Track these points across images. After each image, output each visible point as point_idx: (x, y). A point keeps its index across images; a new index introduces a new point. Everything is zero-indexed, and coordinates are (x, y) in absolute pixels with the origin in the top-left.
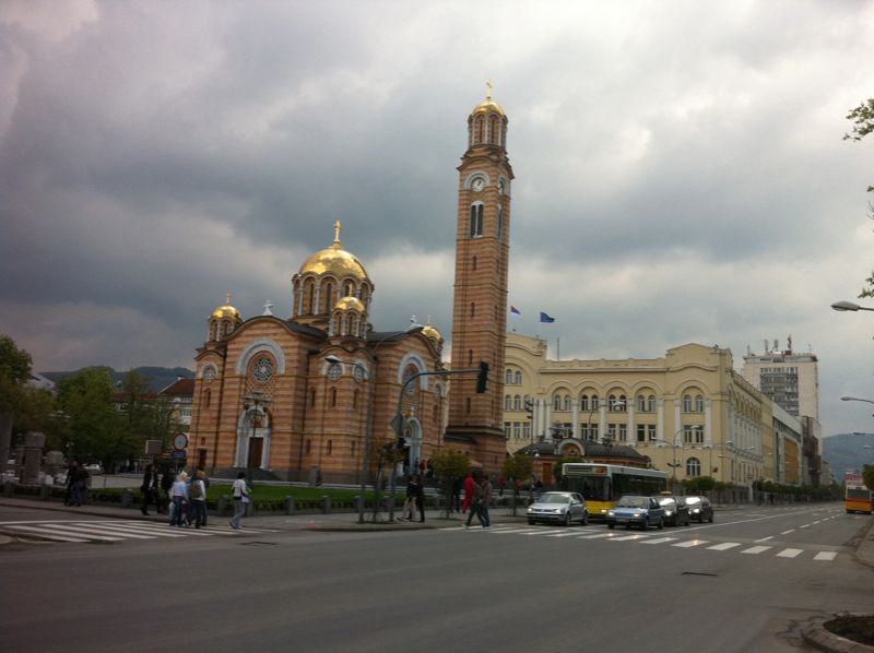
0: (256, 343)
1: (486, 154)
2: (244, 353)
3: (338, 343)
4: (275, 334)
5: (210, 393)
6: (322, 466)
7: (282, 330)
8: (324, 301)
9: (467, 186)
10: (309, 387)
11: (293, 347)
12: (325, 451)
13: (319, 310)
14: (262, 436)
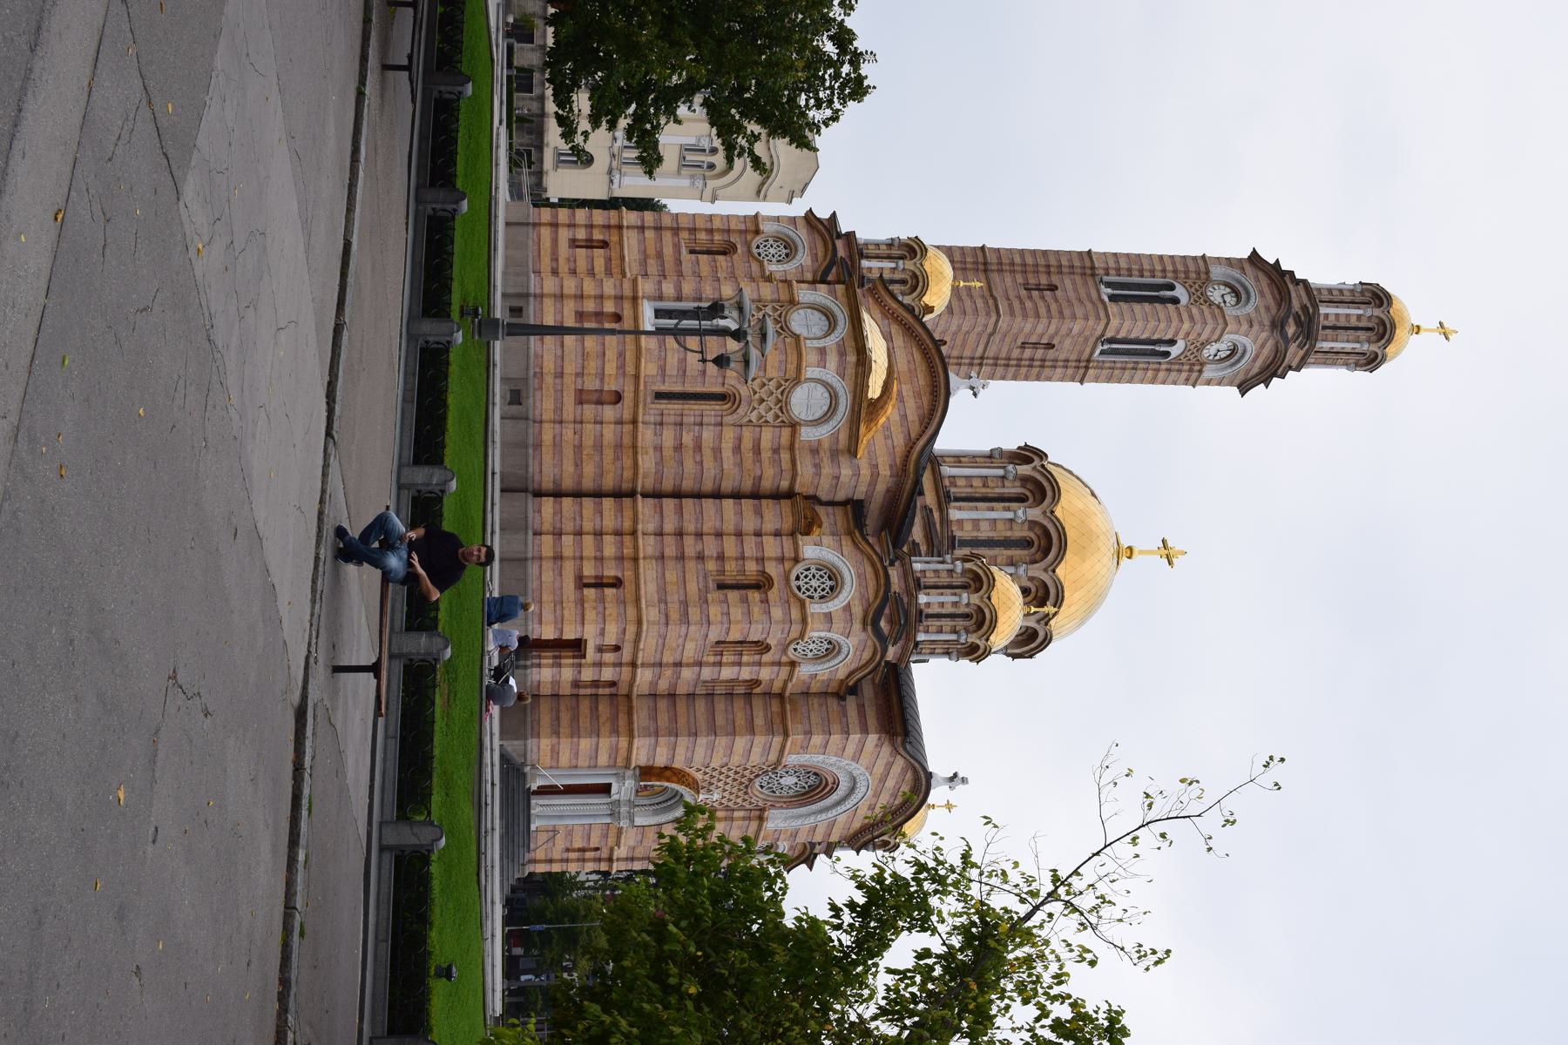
4: (872, 808)
13: (960, 522)
14: (615, 797)
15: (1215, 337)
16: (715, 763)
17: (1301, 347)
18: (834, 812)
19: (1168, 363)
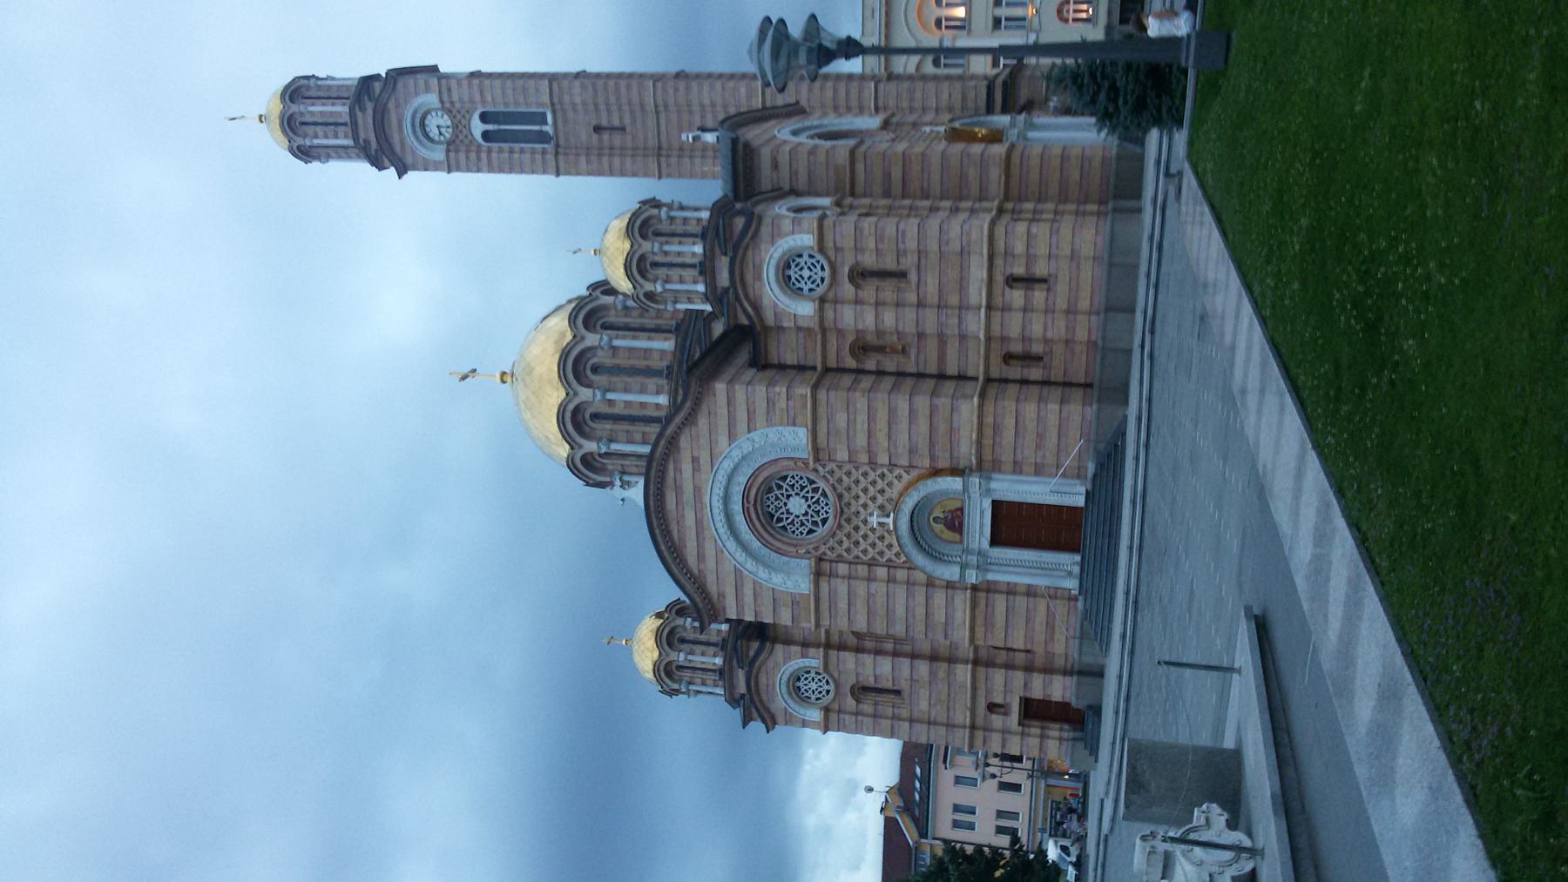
0: (723, 530)
1: (369, 106)
2: (750, 564)
3: (723, 264)
4: (695, 460)
5: (866, 689)
6: (1084, 304)
7: (684, 442)
8: (634, 381)
9: (439, 154)
10: (851, 363)
11: (730, 402)
12: (1039, 295)
14: (987, 504)
15: (452, 155)
16: (882, 572)
17: (367, 142)
18: (736, 454)
19: (476, 109)
